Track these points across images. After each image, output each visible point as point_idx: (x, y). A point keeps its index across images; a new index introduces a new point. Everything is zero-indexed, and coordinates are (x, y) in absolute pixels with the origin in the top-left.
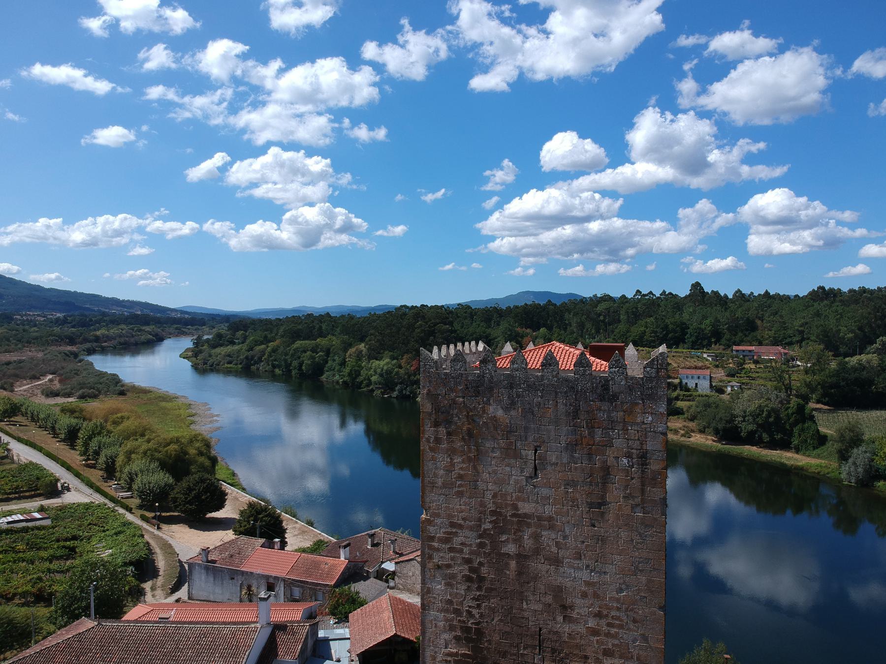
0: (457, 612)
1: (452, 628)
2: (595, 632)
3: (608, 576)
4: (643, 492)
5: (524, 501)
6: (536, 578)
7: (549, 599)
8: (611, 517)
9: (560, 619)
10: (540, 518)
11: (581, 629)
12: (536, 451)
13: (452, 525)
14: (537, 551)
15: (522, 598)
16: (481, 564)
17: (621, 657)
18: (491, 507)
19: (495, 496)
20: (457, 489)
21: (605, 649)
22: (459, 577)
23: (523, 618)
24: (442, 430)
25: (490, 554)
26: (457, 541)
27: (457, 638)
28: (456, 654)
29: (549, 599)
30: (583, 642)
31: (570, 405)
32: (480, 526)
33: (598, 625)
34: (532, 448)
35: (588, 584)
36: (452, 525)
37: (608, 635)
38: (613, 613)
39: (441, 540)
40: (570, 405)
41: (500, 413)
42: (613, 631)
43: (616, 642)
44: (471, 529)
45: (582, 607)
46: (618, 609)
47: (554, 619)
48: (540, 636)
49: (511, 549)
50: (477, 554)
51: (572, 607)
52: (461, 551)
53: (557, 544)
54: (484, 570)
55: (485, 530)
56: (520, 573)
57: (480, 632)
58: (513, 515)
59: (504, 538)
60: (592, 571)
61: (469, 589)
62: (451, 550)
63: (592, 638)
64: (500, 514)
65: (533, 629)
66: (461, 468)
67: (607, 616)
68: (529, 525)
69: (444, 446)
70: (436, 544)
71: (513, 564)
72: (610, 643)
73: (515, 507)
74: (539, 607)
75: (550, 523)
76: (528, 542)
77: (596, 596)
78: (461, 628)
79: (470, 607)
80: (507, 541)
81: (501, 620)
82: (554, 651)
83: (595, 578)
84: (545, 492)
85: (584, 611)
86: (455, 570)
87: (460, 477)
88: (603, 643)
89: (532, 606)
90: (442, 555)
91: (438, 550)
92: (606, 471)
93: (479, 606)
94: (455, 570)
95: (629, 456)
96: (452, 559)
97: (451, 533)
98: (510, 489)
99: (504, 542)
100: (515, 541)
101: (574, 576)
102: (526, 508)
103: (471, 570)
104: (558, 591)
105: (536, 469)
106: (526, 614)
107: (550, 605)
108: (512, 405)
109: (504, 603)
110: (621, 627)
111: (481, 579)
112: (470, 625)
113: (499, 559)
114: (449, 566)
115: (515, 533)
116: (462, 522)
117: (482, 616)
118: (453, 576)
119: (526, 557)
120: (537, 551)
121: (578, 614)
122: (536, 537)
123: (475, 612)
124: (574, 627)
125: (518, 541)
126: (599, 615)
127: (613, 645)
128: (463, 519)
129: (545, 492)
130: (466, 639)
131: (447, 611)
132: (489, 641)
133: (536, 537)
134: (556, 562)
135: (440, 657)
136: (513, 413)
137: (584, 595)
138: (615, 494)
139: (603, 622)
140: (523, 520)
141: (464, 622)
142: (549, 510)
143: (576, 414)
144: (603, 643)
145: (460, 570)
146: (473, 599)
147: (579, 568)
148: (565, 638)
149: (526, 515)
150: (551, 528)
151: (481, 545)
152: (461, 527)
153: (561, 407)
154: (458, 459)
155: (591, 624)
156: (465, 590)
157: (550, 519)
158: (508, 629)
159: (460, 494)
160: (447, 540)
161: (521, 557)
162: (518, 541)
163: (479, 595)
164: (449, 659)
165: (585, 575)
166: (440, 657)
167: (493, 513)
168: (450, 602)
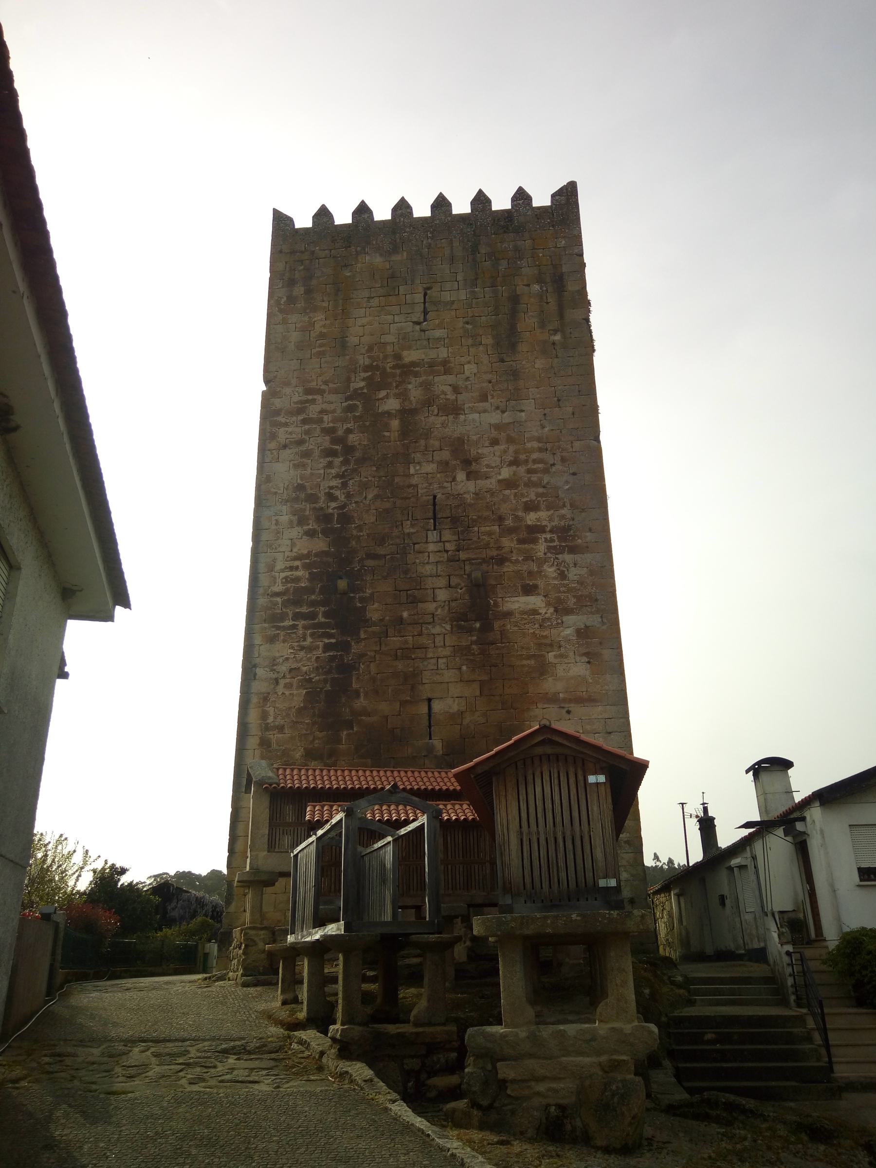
0: (312, 498)
1: (302, 521)
2: (509, 484)
3: (523, 414)
4: (561, 316)
5: (409, 348)
6: (427, 435)
7: (446, 455)
8: (523, 348)
9: (461, 476)
10: (431, 365)
11: (491, 483)
12: (425, 295)
13: (308, 391)
14: (428, 402)
15: (408, 462)
16: (349, 431)
17: (548, 508)
18: (363, 360)
19: (370, 349)
20: (318, 349)
21: (526, 503)
22: (317, 453)
23: (409, 486)
24: (299, 290)
25: (361, 417)
26: (313, 411)
27: (311, 534)
28: (308, 556)
29: (446, 455)
30: (495, 499)
31: (468, 241)
32: (349, 386)
33: (514, 474)
34: (421, 290)
35: (498, 427)
36: (308, 391)
37: (529, 484)
38: (535, 456)
39: (291, 413)
40: (468, 241)
41: (378, 260)
42: (534, 478)
43: (541, 490)
44: (336, 392)
45: (490, 456)
46: (540, 450)
47: (454, 479)
48: (434, 504)
49: (392, 404)
50: (344, 420)
51: (478, 459)
52: (321, 421)
53: (456, 390)
54: (353, 439)
55: (356, 390)
56: (405, 432)
57: (345, 518)
58: (394, 367)
59: (383, 394)
60: (503, 412)
61: (330, 465)
62: (304, 422)
63: (507, 492)
64: (377, 368)
65: (425, 498)
66: (324, 326)
67: (527, 461)
68: (416, 374)
69: (301, 304)
70: (281, 419)
71: (395, 424)
72: (532, 494)
73: (398, 357)
74: (430, 468)
75: (446, 367)
76: (415, 393)
77: (510, 440)
78: (318, 519)
79: (331, 488)
80: (387, 396)
81: (377, 497)
82: (455, 521)
83: (507, 418)
84: (438, 333)
85: (495, 461)
86: (311, 445)
87: (322, 336)
88: (522, 495)
89: (423, 471)
90: (290, 430)
91: (286, 425)
92: (515, 299)
93: (344, 485)
94: (311, 445)
95: (540, 280)
96: (307, 432)
97: (307, 401)
98: (389, 338)
99: (382, 399)
100: (397, 396)
101: (478, 421)
102: (410, 356)
103: (335, 441)
104: (458, 446)
105: (425, 312)
106: (415, 480)
107: (447, 463)
108: (395, 250)
109: (382, 474)
110: (546, 471)
111: (349, 450)
112: (331, 511)
113: (375, 422)
114: (300, 442)
115: (397, 387)
116: (323, 387)
117: (349, 496)
118: (307, 454)
119: (413, 412)
120: (428, 402)
121: (488, 466)
122: (427, 386)
123: (337, 493)
124: (481, 483)
125: (403, 396)
126: (515, 462)
127: (538, 495)
128: (326, 383)
129: (438, 333)
130: (325, 532)
131: (296, 499)
132: (360, 528)
133: (427, 386)
134: (454, 410)
135: (280, 565)
136: (397, 258)
137: (495, 442)
138: (528, 321)
139: (522, 470)
140: (408, 370)
141: (322, 509)
142: (443, 353)
143: (475, 250)
144: (522, 495)
145: (318, 442)
146: (337, 476)
147: (485, 411)
148: (469, 498)
149: (413, 364)
150: (447, 372)
151: (351, 409)
152: (321, 392)
153: (456, 244)
154: (319, 317)
155: (506, 473)
156: (325, 468)
157: (445, 362)
158: (388, 505)
159: (321, 354)
160: (300, 411)
161: (407, 414)
162: (403, 396)
163: (346, 471)
164: (297, 563)
165: (495, 418)
166: (280, 565)
167: (366, 369)
168: (301, 488)
